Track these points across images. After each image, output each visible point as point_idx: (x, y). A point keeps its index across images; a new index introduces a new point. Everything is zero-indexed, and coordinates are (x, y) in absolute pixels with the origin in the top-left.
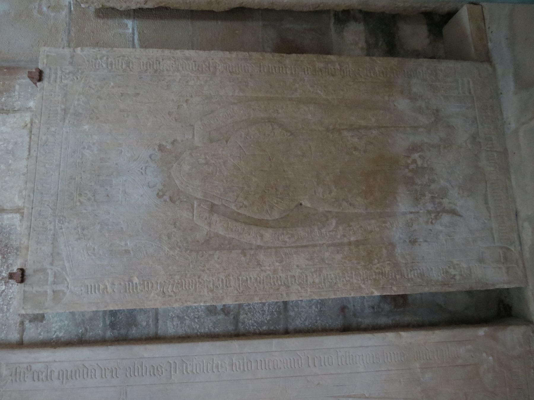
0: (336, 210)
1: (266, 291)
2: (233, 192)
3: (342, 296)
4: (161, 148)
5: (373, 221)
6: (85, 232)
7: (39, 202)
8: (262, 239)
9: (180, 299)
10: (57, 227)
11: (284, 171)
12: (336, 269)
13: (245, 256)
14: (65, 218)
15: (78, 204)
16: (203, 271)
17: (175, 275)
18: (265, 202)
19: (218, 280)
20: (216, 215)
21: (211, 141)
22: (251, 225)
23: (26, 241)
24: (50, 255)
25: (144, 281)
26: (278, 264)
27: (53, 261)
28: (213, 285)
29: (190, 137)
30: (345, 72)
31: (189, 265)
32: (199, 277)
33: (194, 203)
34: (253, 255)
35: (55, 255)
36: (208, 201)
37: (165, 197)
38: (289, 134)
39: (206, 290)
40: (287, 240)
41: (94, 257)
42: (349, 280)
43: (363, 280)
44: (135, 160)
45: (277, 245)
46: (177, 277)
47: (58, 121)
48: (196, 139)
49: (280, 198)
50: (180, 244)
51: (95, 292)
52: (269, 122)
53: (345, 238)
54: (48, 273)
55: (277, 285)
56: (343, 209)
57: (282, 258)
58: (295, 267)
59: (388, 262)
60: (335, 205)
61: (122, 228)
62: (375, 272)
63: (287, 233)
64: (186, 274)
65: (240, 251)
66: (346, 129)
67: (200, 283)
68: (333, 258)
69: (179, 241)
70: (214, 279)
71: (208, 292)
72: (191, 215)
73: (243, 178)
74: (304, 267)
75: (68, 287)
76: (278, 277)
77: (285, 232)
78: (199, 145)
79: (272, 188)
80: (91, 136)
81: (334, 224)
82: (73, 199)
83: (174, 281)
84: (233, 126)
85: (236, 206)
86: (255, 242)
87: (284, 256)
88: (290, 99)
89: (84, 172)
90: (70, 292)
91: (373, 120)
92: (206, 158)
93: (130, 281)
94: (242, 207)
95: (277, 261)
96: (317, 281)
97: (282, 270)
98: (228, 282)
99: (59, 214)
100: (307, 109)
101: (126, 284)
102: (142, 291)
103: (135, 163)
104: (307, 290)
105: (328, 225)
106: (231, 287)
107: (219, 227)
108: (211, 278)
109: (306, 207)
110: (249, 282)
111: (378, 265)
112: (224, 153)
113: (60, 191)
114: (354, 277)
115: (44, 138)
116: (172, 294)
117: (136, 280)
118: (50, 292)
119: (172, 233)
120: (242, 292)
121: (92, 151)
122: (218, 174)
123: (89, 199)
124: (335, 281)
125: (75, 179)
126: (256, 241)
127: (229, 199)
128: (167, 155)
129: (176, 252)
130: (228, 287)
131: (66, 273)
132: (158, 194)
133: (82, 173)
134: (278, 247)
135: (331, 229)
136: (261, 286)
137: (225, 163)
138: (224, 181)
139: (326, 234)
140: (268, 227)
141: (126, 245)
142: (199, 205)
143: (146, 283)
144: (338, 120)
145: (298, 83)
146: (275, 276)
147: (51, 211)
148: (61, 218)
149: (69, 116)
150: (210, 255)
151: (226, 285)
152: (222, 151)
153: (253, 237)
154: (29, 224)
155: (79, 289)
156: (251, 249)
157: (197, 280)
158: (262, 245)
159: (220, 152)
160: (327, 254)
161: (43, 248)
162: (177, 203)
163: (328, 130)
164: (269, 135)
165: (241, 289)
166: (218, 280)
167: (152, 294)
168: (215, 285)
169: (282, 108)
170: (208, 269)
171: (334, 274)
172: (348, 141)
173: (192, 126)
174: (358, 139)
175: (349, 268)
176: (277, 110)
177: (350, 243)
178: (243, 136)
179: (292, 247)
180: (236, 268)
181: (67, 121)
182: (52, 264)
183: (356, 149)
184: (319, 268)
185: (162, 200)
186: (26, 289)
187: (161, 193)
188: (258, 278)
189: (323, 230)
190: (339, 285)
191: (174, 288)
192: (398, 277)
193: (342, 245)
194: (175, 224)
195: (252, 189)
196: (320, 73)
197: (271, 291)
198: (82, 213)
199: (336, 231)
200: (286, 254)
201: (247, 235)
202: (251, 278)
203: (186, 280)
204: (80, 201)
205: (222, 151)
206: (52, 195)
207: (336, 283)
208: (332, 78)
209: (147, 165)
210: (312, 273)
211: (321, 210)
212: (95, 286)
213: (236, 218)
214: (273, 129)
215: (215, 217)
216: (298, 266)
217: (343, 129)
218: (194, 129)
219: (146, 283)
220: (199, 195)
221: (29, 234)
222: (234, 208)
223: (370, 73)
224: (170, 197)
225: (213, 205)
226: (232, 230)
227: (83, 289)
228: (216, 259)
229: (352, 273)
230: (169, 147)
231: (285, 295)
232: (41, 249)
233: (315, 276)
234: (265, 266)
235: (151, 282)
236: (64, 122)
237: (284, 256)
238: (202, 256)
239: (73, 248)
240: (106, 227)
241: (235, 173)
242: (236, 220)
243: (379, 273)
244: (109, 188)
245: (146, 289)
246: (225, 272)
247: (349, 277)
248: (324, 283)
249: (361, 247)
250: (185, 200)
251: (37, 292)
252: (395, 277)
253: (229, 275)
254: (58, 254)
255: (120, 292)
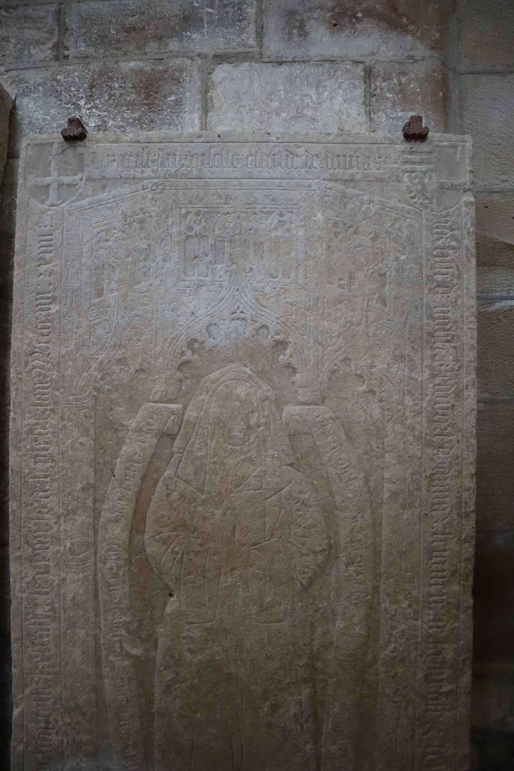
0: (159, 660)
1: (24, 522)
2: (195, 474)
3: (13, 651)
4: (281, 345)
5: (137, 723)
6: (136, 225)
7: (189, 152)
8: (110, 521)
9: (21, 379)
10: (146, 181)
11: (233, 569)
12: (56, 646)
13: (83, 489)
14: (161, 193)
15: (183, 211)
16: (62, 418)
17: (59, 372)
18: (175, 529)
19: (47, 443)
20: (156, 441)
21: (293, 436)
22: (137, 502)
23: (128, 139)
24: (103, 175)
25: (52, 321)
26: (68, 545)
27: (94, 180)
28: (40, 434)
29: (300, 398)
30: (435, 702)
31: (74, 395)
32: (52, 411)
33: (177, 403)
34: (85, 503)
35: (103, 182)
36: (180, 428)
37: (189, 353)
38: (304, 582)
39: (32, 421)
40: (108, 566)
41: (94, 241)
42: (37, 668)
43: (38, 693)
44: (257, 300)
45: (99, 547)
46: (54, 375)
47: (331, 171)
48: (298, 408)
49: (182, 558)
50: (108, 378)
51: (41, 247)
52: (331, 547)
53: (108, 669)
54: (76, 175)
55: (35, 541)
56: (161, 671)
57: (78, 555)
58: (63, 575)
59: (65, 741)
60: (168, 658)
61: (139, 282)
62: (49, 716)
63: (119, 567)
64: (58, 390)
65: (92, 481)
66: (315, 693)
67: (44, 413)
68: (74, 643)
69: (113, 377)
70: (49, 435)
71: (29, 424)
72: (156, 399)
73: (220, 493)
74: (62, 591)
75: (53, 205)
76: (47, 545)
77: (122, 562)
78: (284, 414)
79: (201, 545)
80: (305, 225)
81: (135, 652)
82: (191, 203)
83: (49, 370)
84: (322, 477)
85: (170, 478)
86: (106, 507)
87: (81, 556)
88: (376, 589)
89: (239, 217)
90: (45, 209)
91: (334, 749)
92: (259, 426)
93: (54, 299)
94: (168, 489)
95: (72, 544)
96: (39, 611)
97: (58, 551)
98: (42, 458)
99: (167, 183)
100: (356, 620)
101: (49, 292)
102: (37, 319)
103: (254, 301)
104: (25, 592)
105: (133, 641)
106: (35, 463)
107: (133, 447)
108: (50, 430)
109: (165, 604)
110: (41, 494)
111: (61, 723)
112: (269, 459)
113: (206, 182)
114: (43, 676)
115: (301, 151)
116: (30, 367)
117: (54, 308)
118: (48, 180)
119: (127, 365)
120: (25, 482)
121: (276, 229)
122: (230, 447)
123: (190, 228)
124: (37, 642)
125: (226, 203)
126: (108, 509)
127: (182, 465)
128: (268, 354)
129: (95, 373)
130: (35, 458)
131: (73, 202)
132: (195, 340)
133: (236, 214)
134: (96, 548)
135: (124, 645)
136: (34, 515)
137: (250, 460)
138: (215, 459)
139: (117, 636)
140: (130, 532)
141: (112, 291)
142: (173, 413)
143: (49, 324)
144: (335, 680)
145: (409, 606)
146: (49, 539)
147: (173, 170)
148: (160, 187)
149: (341, 187)
150: (87, 430)
151: (38, 455)
152: (273, 457)
153: (114, 506)
154: (155, 140)
155: (47, 223)
156: (95, 501)
157: (49, 408)
158: (102, 520)
159: (270, 452)
160: (82, 633)
161: (115, 164)
162: (178, 374)
163: (314, 657)
164: (303, 544)
165: (31, 480)
166: (47, 443)
167: (31, 335)
168: (40, 437)
169: (358, 573)
170: (64, 426)
171: (49, 642)
172: (291, 694)
173: (323, 401)
174: (295, 714)
175: (58, 669)
176: (353, 563)
177: (99, 677)
178: (302, 496)
179: (95, 574)
180: (63, 473)
181: (330, 184)
182: (89, 179)
183: (275, 708)
184: (59, 618)
185: (185, 349)
186: (55, 146)
187: (196, 346)
188: (46, 510)
189: (123, 631)
190: (30, 649)
191: (39, 370)
192: (40, 756)
193: (98, 663)
194: (142, 370)
195: (200, 508)
196: (432, 651)
197: (25, 531)
198: (167, 217)
199: (120, 654)
200: (84, 561)
201: (119, 494)
202: (47, 497)
203: (50, 390)
204: (187, 213)
205: (273, 457)
206: (200, 170)
207: (34, 643)
208: (420, 674)
209: (249, 321)
210: (51, 603)
211: (160, 630)
212: (51, 246)
213: (149, 477)
214: (314, 553)
215: (151, 441)
216: (64, 579)
217: (314, 687)
218: (317, 404)
219: (49, 324)
220: (191, 413)
221: (138, 142)
223: (434, 754)
224: (189, 362)
225: (172, 437)
226: (127, 469)
227: (48, 227)
228: (80, 440)
229: (49, 673)
230: (282, 358)
231: (18, 554)
232: (114, 160)
233: (47, 608)
234: (65, 522)
235: (49, 333)
236: (329, 180)
237: (81, 556)
238: (86, 417)
239: (110, 208)
240: (142, 258)
241: (230, 478)
242: (144, 478)
243: (47, 722)
244: (209, 258)
245: (40, 325)
246: (58, 454)
247: (43, 668)
248: (34, 624)
249: (92, 695)
250: (184, 388)
251: (50, 161)
252: (39, 752)
253: (53, 461)
254: (104, 187)
255: (38, 285)
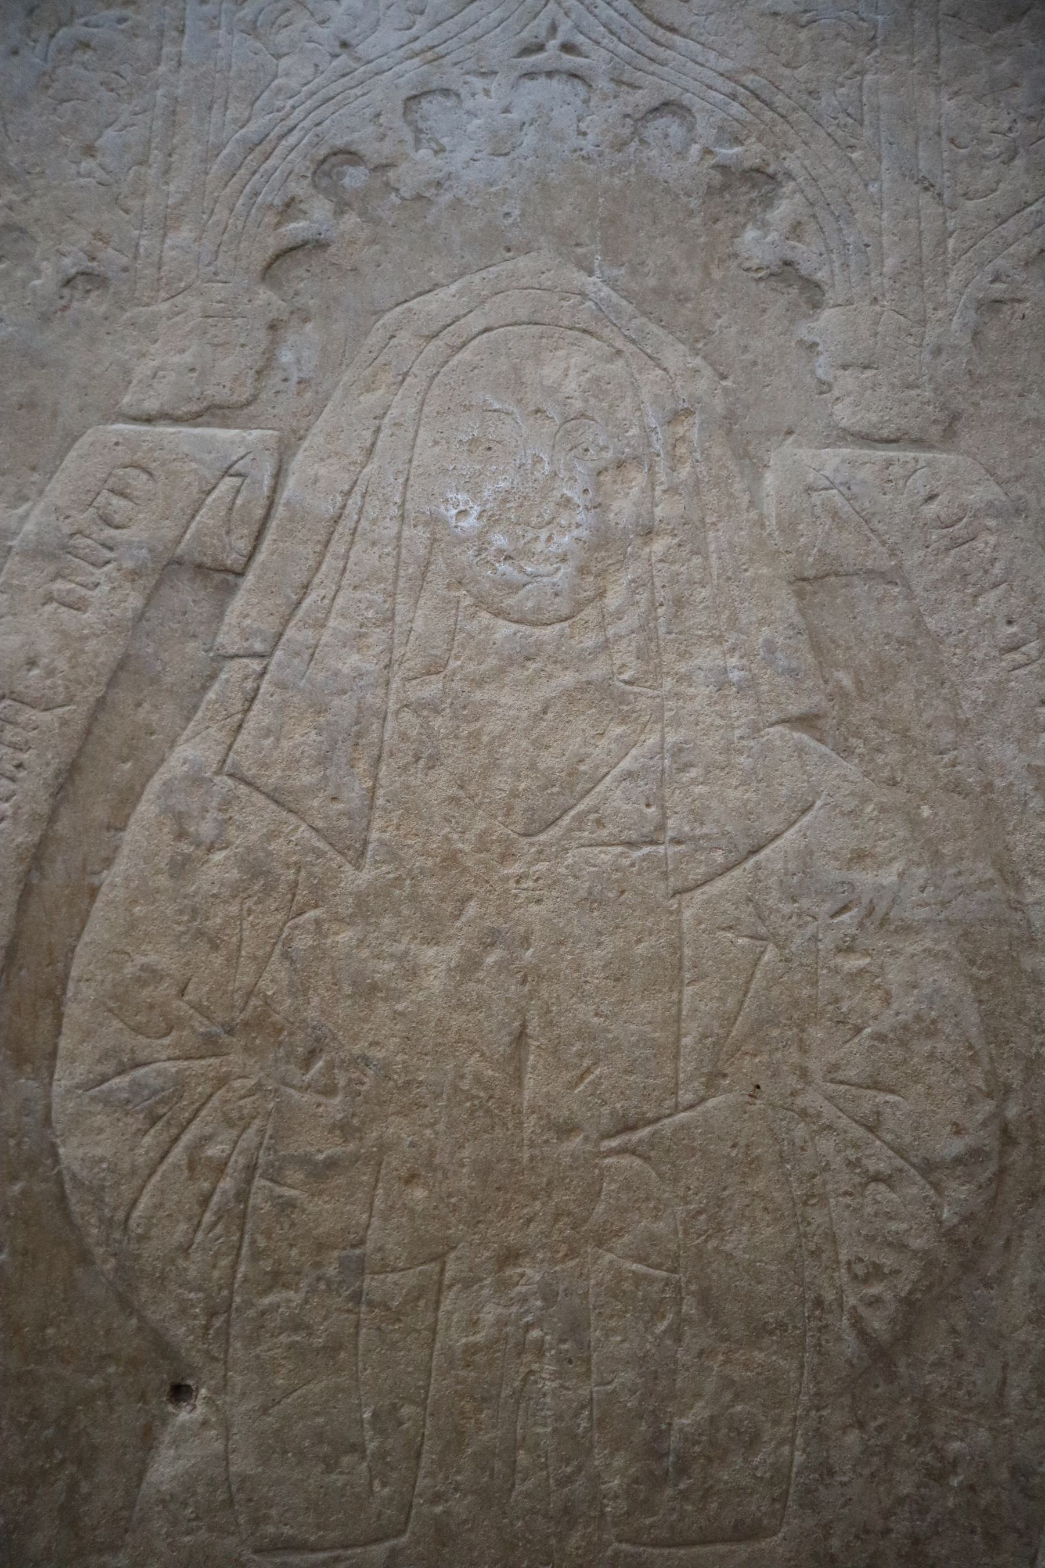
2: (323, 760)
11: (510, 1256)
18: (210, 1045)
20: (135, 601)
36: (259, 537)
38: (878, 1324)
49: (242, 1195)
52: (1007, 1137)
72: (151, 405)
73: (451, 859)
79: (344, 1129)
84: (956, 787)
85: (197, 780)
92: (648, 533)
94: (181, 835)
109: (147, 1440)
112: (702, 691)
122: (504, 629)
127: (260, 716)
132: (350, 155)
138: (432, 688)
162: (264, 294)
178: (864, 878)
187: (354, 178)
195: (346, 936)
209: (603, 83)
214: (927, 1168)
215: (109, 598)
218: (919, 443)
222: (189, 753)
224: (320, 245)
225: (221, 577)
241: (502, 783)
242: (65, 783)
